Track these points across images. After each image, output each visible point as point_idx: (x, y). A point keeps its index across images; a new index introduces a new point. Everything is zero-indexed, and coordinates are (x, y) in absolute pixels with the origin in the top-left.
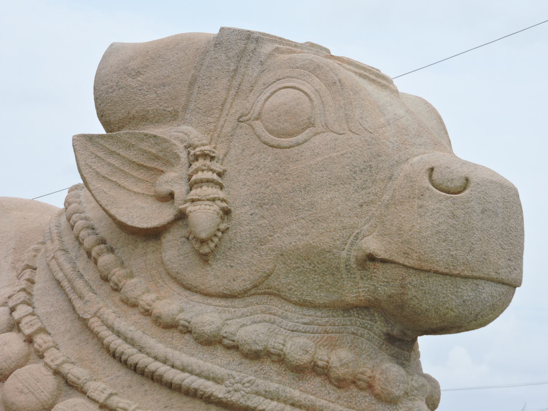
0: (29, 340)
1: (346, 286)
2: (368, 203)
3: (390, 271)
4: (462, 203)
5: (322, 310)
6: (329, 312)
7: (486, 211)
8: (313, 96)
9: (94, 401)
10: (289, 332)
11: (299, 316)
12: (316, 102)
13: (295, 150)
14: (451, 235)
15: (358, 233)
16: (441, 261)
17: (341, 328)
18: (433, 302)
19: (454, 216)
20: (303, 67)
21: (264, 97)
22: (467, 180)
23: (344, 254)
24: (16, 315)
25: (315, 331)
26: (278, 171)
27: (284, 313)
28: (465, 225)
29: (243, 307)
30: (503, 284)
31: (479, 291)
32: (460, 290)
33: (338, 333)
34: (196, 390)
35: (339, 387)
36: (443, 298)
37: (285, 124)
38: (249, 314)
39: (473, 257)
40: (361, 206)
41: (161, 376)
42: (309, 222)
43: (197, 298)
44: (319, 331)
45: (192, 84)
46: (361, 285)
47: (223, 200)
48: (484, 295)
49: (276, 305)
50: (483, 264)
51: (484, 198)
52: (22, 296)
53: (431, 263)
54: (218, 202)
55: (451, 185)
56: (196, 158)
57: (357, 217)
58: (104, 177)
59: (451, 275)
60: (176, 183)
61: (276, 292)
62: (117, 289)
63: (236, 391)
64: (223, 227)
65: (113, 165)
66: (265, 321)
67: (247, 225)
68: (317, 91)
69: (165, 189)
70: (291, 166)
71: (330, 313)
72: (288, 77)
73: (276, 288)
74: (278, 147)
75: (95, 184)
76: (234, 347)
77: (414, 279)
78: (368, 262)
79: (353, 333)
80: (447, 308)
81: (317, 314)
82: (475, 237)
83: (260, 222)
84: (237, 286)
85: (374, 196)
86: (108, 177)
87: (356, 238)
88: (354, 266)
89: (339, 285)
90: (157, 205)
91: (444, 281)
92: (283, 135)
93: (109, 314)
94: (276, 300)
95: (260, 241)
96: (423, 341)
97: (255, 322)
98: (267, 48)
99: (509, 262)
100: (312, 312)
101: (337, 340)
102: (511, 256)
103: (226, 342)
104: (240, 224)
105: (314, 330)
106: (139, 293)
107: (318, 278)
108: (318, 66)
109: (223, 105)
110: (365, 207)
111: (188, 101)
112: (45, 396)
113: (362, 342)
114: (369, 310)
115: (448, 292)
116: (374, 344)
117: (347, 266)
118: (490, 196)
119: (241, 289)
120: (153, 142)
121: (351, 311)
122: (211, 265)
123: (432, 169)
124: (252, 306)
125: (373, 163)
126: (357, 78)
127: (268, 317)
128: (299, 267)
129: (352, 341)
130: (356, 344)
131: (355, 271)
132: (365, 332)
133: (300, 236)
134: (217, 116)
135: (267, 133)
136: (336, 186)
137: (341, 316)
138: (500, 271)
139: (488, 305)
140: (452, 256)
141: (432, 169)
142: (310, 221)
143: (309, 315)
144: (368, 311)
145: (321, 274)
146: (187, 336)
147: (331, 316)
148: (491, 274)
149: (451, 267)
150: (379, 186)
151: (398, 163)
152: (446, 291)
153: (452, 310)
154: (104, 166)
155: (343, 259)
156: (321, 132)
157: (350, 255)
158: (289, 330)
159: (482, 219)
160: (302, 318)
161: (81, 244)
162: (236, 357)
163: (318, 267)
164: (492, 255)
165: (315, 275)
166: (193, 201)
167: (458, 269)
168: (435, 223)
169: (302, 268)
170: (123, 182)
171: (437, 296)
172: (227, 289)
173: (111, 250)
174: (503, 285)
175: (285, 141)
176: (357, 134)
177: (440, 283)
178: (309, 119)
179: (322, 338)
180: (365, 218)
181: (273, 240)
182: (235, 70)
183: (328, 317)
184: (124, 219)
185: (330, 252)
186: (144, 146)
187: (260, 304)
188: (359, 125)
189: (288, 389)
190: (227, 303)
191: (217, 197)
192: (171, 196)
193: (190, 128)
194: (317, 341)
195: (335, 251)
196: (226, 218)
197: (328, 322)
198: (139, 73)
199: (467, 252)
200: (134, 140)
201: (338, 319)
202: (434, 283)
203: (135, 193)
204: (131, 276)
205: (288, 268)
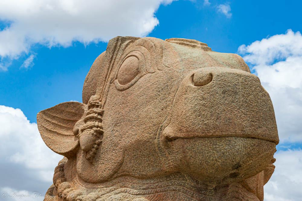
1: (162, 161)
4: (208, 89)
5: (154, 179)
6: (158, 180)
7: (227, 91)
8: (139, 57)
10: (134, 196)
11: (141, 185)
13: (130, 89)
14: (203, 111)
15: (161, 126)
16: (199, 129)
17: (166, 188)
18: (203, 158)
19: (204, 99)
22: (211, 75)
23: (156, 141)
25: (150, 192)
26: (123, 103)
27: (132, 185)
28: (212, 103)
29: (111, 186)
30: (253, 138)
31: (232, 145)
32: (217, 146)
33: (164, 191)
36: (207, 154)
37: (126, 76)
38: (113, 189)
39: (220, 122)
40: (163, 110)
42: (137, 127)
44: (152, 192)
46: (170, 158)
48: (238, 147)
50: (230, 126)
51: (224, 84)
53: (194, 132)
57: (160, 117)
58: (50, 131)
59: (208, 137)
60: (81, 124)
61: (127, 173)
64: (97, 142)
65: (55, 123)
66: (122, 192)
67: (109, 138)
68: (142, 54)
70: (129, 98)
71: (159, 180)
72: (131, 52)
73: (127, 171)
77: (188, 145)
78: (168, 142)
79: (174, 190)
80: (213, 160)
81: (151, 182)
82: (220, 109)
83: (115, 134)
85: (169, 102)
86: (52, 130)
88: (163, 147)
89: (158, 161)
91: (205, 142)
92: (126, 82)
94: (129, 178)
95: (115, 145)
97: (116, 193)
99: (252, 123)
100: (148, 181)
101: (164, 196)
102: (254, 119)
104: (107, 138)
105: (149, 192)
106: (62, 189)
107: (146, 159)
108: (145, 41)
109: (106, 78)
110: (165, 110)
113: (180, 195)
114: (180, 173)
115: (210, 149)
116: (188, 195)
117: (159, 148)
118: (229, 82)
119: (108, 175)
120: (72, 106)
121: (171, 176)
122: (94, 165)
124: (116, 184)
125: (169, 83)
127: (123, 189)
128: (135, 155)
129: (173, 195)
130: (176, 197)
131: (164, 150)
132: (181, 188)
133: (133, 136)
134: (103, 84)
135: (119, 84)
136: (150, 102)
137: (165, 181)
138: (245, 129)
139: (243, 153)
140: (205, 124)
142: (137, 126)
143: (146, 184)
144: (180, 174)
145: (147, 157)
147: (159, 182)
148: (237, 132)
149: (206, 132)
150: (172, 95)
152: (208, 148)
153: (216, 160)
154: (51, 125)
155: (156, 144)
156: (144, 75)
157: (159, 140)
158: (135, 195)
159: (224, 97)
160: (142, 186)
163: (145, 152)
164: (236, 119)
165: (145, 158)
167: (211, 132)
168: (193, 106)
169: (137, 155)
171: (203, 153)
172: (102, 177)
174: (252, 139)
175: (126, 86)
176: (161, 70)
177: (203, 144)
178: (137, 70)
179: (154, 196)
180: (165, 116)
181: (121, 142)
182: (112, 58)
183: (157, 182)
185: (148, 141)
186: (68, 110)
187: (120, 182)
188: (163, 65)
190: (103, 185)
191: (93, 125)
194: (151, 198)
195: (151, 140)
196: (101, 137)
197: (157, 185)
199: (215, 119)
200: (63, 107)
201: (163, 183)
202: (199, 144)
205: (130, 157)
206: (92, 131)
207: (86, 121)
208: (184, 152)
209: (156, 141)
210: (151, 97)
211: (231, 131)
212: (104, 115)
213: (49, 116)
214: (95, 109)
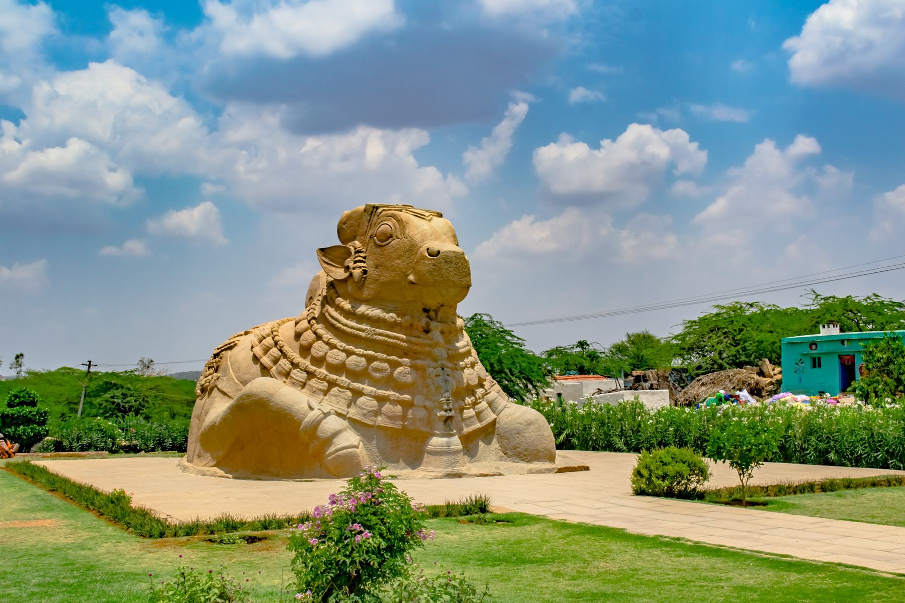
2: (410, 263)
63: (369, 334)
112: (310, 341)
151: (420, 247)
182: (370, 220)
198: (346, 223)
207: (355, 262)
210: (401, 255)
212: (367, 258)
214: (360, 254)
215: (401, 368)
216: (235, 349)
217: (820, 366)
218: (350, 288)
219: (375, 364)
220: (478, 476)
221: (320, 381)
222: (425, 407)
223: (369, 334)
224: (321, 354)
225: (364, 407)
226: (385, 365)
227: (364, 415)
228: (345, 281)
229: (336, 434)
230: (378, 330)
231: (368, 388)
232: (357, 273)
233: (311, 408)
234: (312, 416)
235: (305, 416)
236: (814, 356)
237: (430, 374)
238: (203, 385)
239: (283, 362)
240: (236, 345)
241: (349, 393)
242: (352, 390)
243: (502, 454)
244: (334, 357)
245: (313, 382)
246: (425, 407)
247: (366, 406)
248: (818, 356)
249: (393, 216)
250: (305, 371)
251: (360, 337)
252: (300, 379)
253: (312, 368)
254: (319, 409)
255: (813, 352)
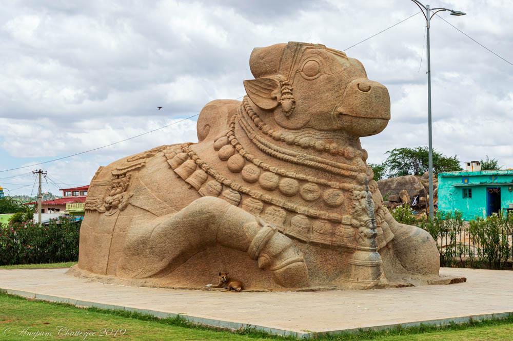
0: (234, 147)
3: (347, 118)
9: (256, 165)
12: (321, 64)
13: (315, 81)
20: (316, 53)
21: (303, 64)
22: (370, 87)
23: (332, 113)
24: (230, 139)
34: (288, 160)
35: (333, 156)
41: (276, 156)
43: (286, 130)
45: (280, 61)
47: (292, 98)
49: (312, 131)
52: (231, 133)
54: (291, 99)
55: (365, 89)
56: (283, 85)
62: (261, 129)
63: (301, 159)
64: (293, 107)
69: (274, 96)
74: (309, 80)
75: (252, 96)
76: (299, 145)
84: (299, 126)
87: (336, 108)
90: (271, 101)
93: (259, 137)
96: (361, 139)
98: (304, 47)
103: (296, 144)
104: (299, 106)
111: (280, 67)
123: (359, 84)
126: (334, 55)
127: (309, 135)
141: (359, 84)
143: (322, 133)
146: (284, 143)
151: (348, 83)
161: (249, 115)
162: (300, 148)
166: (283, 99)
170: (260, 95)
173: (258, 117)
175: (311, 78)
182: (294, 56)
184: (261, 107)
186: (266, 82)
189: (317, 157)
192: (275, 99)
193: (281, 75)
198: (263, 58)
202: (361, 121)
203: (264, 98)
204: (265, 124)
206: (290, 101)
207: (283, 94)
208: (352, 123)
209: (332, 113)
210: (329, 89)
211: (377, 116)
213: (253, 84)
215: (331, 190)
216: (144, 171)
217: (470, 196)
218: (278, 116)
219: (307, 186)
220: (397, 287)
221: (256, 201)
222: (351, 225)
223: (301, 159)
224: (254, 176)
225: (298, 224)
226: (315, 187)
227: (299, 232)
228: (271, 111)
229: (285, 249)
230: (309, 156)
231: (302, 208)
232: (286, 104)
233: (261, 225)
234: (262, 233)
235: (256, 232)
236: (465, 188)
237: (356, 196)
238: (112, 202)
239: (211, 182)
240: (143, 166)
241: (284, 213)
242: (287, 210)
243: (402, 267)
244: (268, 179)
245: (247, 201)
246: (351, 225)
247: (300, 224)
248: (469, 188)
249: (320, 54)
250: (238, 192)
251: (292, 162)
252: (235, 199)
253: (246, 188)
254: (268, 226)
255: (466, 185)
